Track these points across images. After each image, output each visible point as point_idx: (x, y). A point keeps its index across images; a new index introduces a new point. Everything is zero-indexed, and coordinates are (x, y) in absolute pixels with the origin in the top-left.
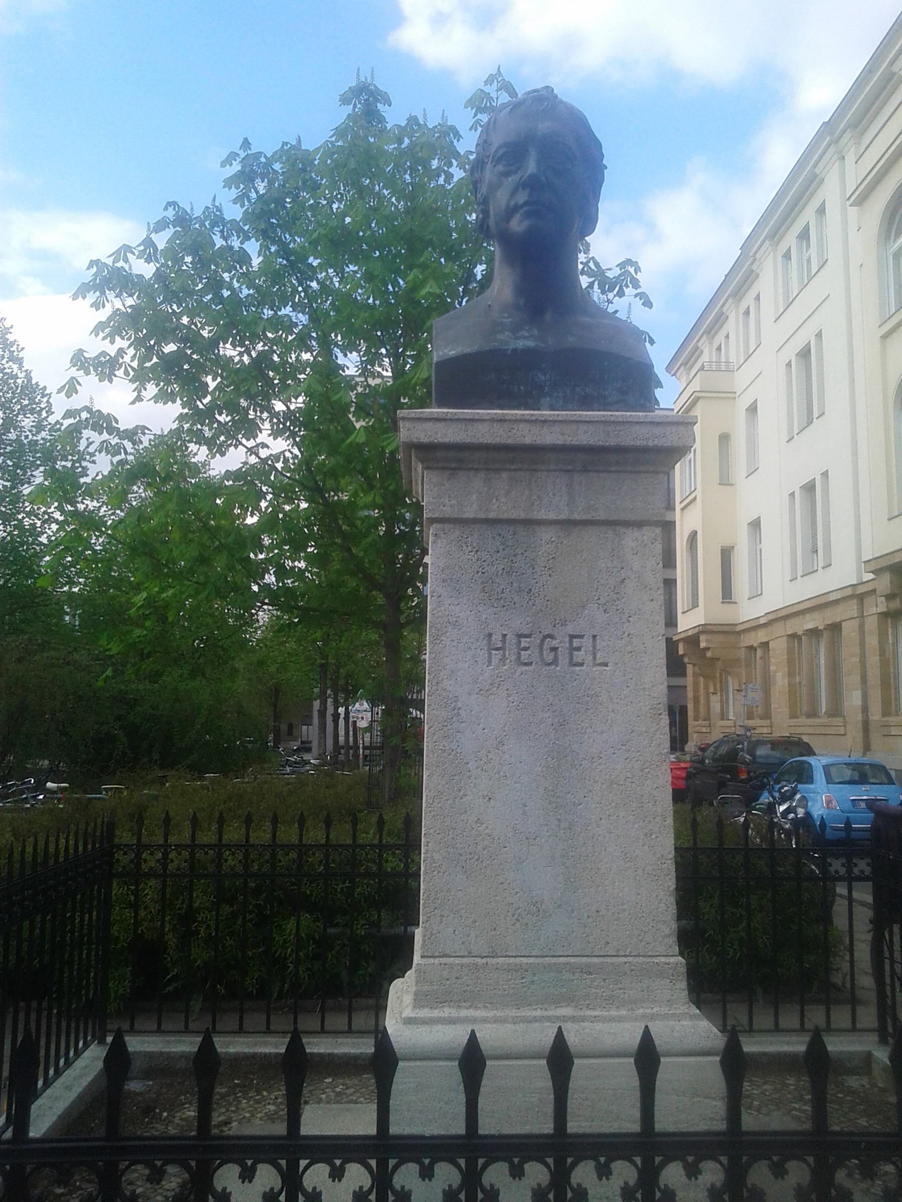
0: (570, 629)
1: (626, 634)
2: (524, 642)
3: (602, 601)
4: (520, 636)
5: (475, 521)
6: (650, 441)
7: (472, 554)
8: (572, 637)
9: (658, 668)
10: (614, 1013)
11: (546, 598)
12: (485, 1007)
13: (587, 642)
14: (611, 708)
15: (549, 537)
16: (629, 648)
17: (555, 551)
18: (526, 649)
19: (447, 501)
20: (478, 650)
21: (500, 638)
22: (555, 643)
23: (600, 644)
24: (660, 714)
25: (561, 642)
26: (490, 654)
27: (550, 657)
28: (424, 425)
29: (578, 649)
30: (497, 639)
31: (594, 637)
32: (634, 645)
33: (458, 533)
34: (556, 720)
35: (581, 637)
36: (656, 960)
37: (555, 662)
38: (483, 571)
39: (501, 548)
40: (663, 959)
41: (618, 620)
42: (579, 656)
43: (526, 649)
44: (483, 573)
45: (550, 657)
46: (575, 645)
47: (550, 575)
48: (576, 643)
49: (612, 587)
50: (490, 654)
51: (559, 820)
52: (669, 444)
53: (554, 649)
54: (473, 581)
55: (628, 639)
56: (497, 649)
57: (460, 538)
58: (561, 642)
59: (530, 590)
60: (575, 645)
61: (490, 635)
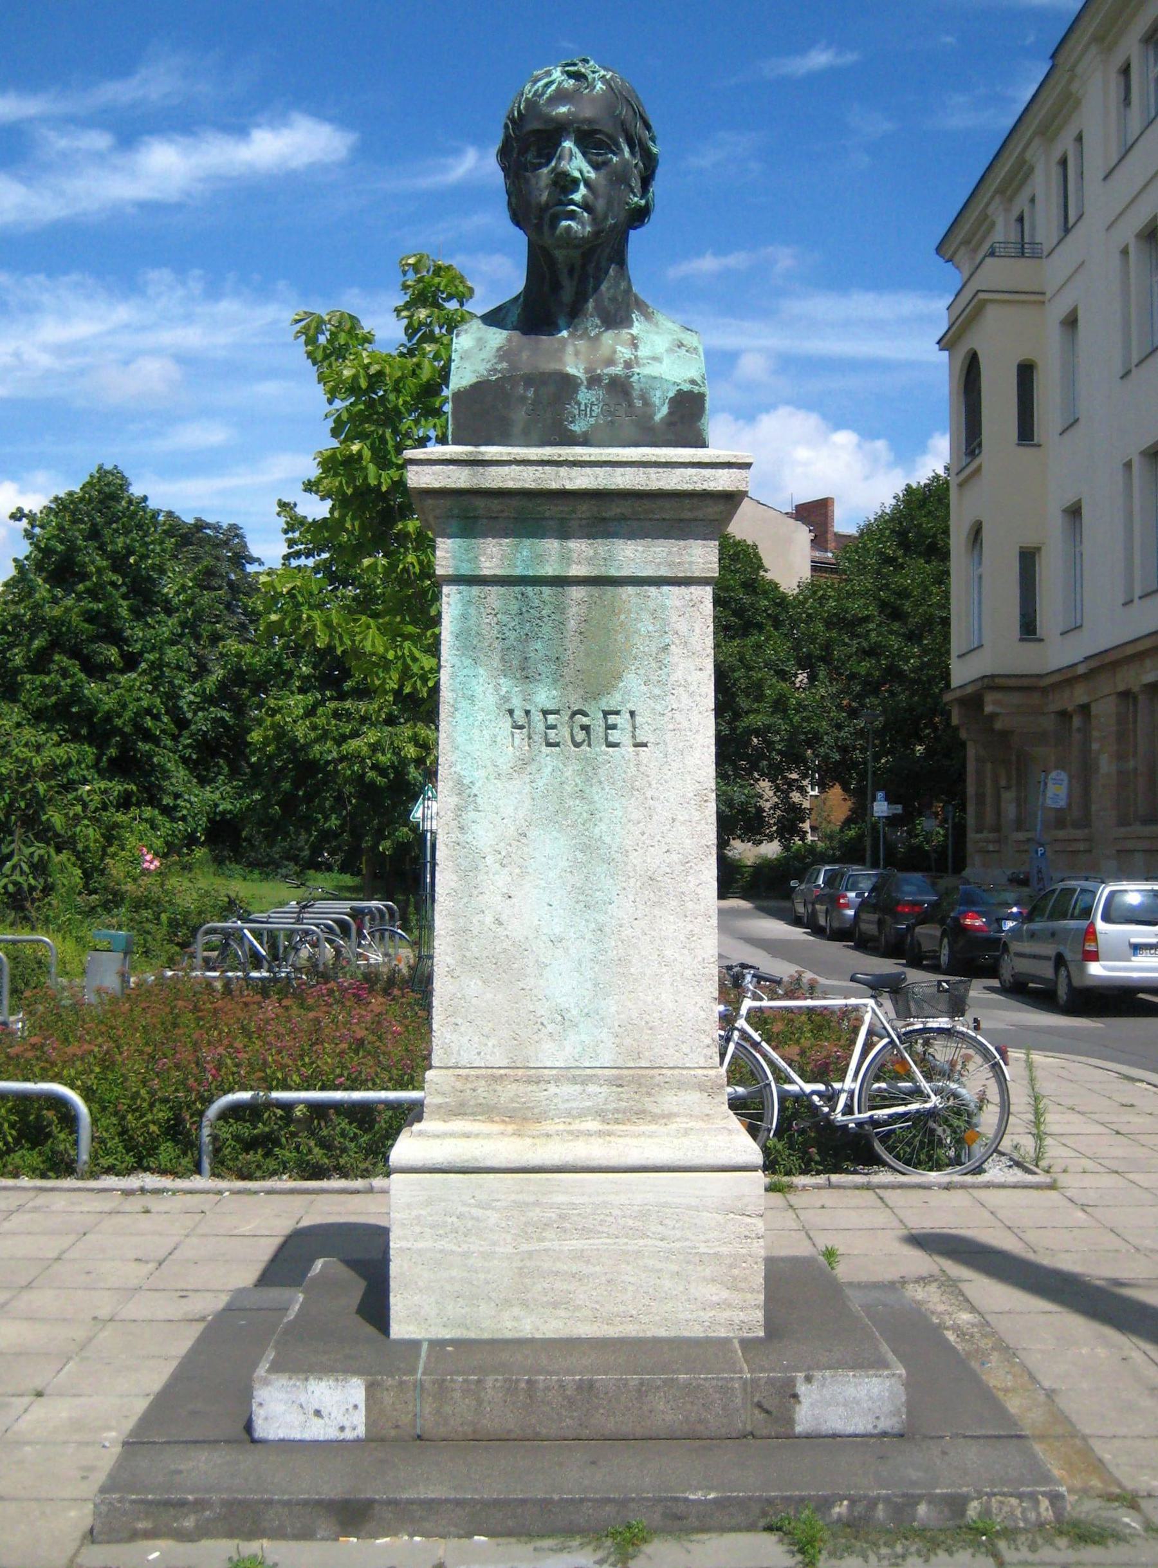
2: (551, 719)
4: (545, 713)
8: (606, 714)
10: (643, 1128)
12: (503, 1121)
14: (649, 794)
15: (579, 596)
16: (671, 727)
18: (553, 727)
21: (523, 714)
22: (585, 721)
23: (639, 720)
26: (513, 734)
29: (614, 727)
30: (519, 714)
31: (632, 713)
35: (617, 713)
36: (692, 1072)
40: (700, 1072)
42: (614, 736)
43: (553, 727)
45: (580, 736)
46: (610, 722)
48: (612, 719)
50: (513, 734)
51: (587, 921)
52: (720, 488)
53: (586, 728)
55: (670, 714)
56: (521, 727)
60: (610, 722)
61: (511, 712)
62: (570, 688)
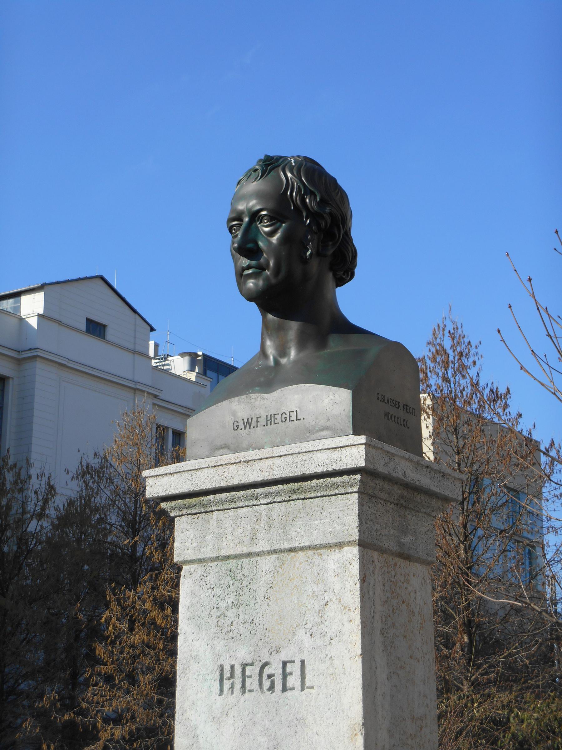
0: (284, 656)
1: (329, 656)
3: (309, 626)
5: (212, 560)
6: (330, 466)
7: (210, 591)
9: (355, 689)
11: (265, 627)
13: (298, 665)
17: (272, 580)
19: (190, 544)
20: (213, 681)
24: (356, 734)
25: (275, 669)
27: (267, 684)
28: (162, 480)
32: (335, 667)
33: (200, 573)
34: (271, 744)
37: (272, 688)
38: (218, 606)
39: (231, 583)
41: (321, 643)
43: (250, 677)
44: (217, 608)
47: (268, 605)
49: (317, 611)
53: (269, 676)
54: (210, 616)
57: (202, 577)
58: (275, 669)
59: (253, 620)
62: (260, 643)
